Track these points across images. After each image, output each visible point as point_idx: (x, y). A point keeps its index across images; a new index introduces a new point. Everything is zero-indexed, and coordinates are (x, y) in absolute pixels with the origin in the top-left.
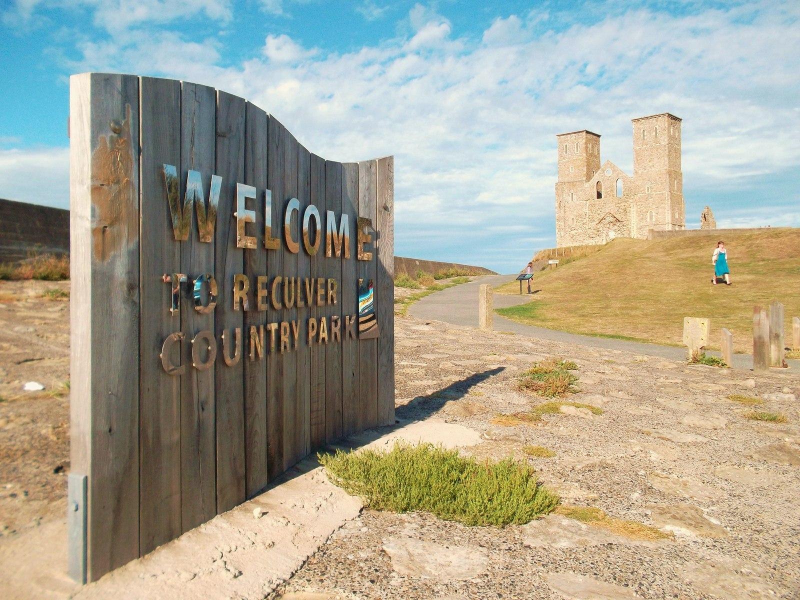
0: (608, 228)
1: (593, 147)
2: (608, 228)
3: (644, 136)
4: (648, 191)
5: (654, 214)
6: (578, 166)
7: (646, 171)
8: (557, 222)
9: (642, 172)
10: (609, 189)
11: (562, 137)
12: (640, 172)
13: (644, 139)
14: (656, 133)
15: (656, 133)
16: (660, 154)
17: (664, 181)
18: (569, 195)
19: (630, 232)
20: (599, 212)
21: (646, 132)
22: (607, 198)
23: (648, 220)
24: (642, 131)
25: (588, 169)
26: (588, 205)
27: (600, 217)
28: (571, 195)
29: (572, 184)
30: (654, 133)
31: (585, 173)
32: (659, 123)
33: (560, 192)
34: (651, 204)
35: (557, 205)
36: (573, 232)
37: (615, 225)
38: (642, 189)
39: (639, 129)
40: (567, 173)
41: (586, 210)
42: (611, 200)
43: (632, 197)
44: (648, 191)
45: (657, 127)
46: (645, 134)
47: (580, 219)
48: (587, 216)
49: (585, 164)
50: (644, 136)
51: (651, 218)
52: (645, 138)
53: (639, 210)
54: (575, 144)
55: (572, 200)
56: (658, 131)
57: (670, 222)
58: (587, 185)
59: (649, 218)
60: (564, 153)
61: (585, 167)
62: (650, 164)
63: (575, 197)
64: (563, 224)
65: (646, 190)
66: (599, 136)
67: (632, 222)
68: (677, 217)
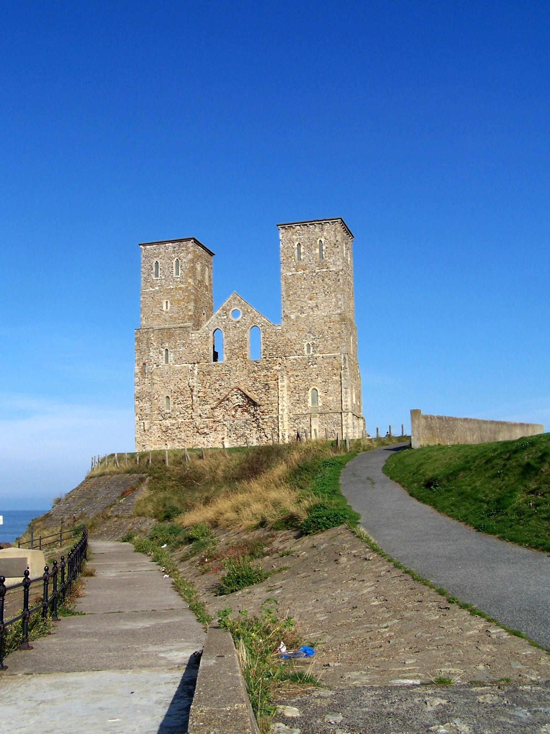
0: (233, 416)
1: (203, 270)
2: (233, 416)
3: (299, 253)
4: (309, 351)
5: (319, 394)
7: (303, 316)
8: (137, 403)
9: (297, 317)
10: (237, 345)
11: (148, 247)
12: (293, 317)
13: (299, 259)
14: (321, 250)
15: (321, 250)
16: (330, 286)
18: (160, 352)
23: (310, 404)
24: (296, 246)
25: (196, 308)
26: (196, 372)
27: (219, 396)
28: (164, 353)
29: (167, 334)
30: (318, 251)
33: (144, 346)
34: (314, 375)
35: (137, 369)
36: (168, 422)
38: (298, 347)
39: (291, 241)
40: (157, 311)
41: (194, 382)
42: (240, 364)
43: (280, 360)
45: (323, 240)
46: (302, 251)
47: (181, 398)
48: (195, 393)
50: (299, 253)
51: (315, 401)
52: (302, 257)
53: (291, 385)
54: (174, 262)
55: (167, 361)
56: (324, 248)
57: (350, 410)
58: (194, 336)
59: (310, 400)
60: (153, 276)
61: (192, 304)
62: (312, 303)
63: (171, 356)
64: (147, 405)
65: (305, 349)
67: (280, 407)
68: (354, 402)
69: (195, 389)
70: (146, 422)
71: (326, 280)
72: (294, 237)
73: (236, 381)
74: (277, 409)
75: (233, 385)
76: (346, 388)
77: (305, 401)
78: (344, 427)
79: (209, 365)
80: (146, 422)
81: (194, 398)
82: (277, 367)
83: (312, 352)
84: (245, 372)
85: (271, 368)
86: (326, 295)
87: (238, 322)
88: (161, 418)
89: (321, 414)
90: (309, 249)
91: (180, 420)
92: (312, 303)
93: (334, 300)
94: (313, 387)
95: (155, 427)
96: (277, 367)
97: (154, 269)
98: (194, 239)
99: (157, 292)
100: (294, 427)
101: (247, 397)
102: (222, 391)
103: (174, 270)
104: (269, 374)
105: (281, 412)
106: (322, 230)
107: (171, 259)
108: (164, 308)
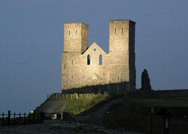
3: (116, 31)
6: (77, 44)
14: (122, 30)
15: (122, 30)
17: (126, 59)
20: (88, 73)
21: (117, 29)
22: (94, 65)
24: (115, 28)
30: (121, 30)
31: (81, 48)
32: (124, 25)
45: (123, 27)
46: (117, 30)
49: (81, 43)
50: (116, 31)
52: (116, 32)
55: (72, 64)
56: (123, 29)
58: (81, 56)
60: (68, 35)
63: (74, 62)
69: (81, 73)
71: (124, 40)
72: (114, 25)
75: (94, 73)
86: (123, 45)
92: (119, 48)
97: (69, 32)
103: (75, 33)
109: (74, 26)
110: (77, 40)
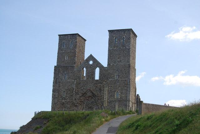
3: (115, 41)
4: (116, 78)
9: (113, 65)
14: (123, 40)
16: (126, 54)
19: (103, 104)
36: (63, 101)
37: (92, 98)
44: (116, 78)
45: (124, 37)
48: (74, 91)
50: (115, 41)
56: (125, 40)
63: (67, 77)
66: (85, 40)
67: (105, 98)
70: (56, 100)
73: (89, 87)
74: (103, 98)
75: (88, 88)
76: (129, 92)
77: (114, 96)
78: (127, 106)
79: (80, 81)
80: (56, 100)
81: (74, 92)
82: (104, 83)
83: (117, 78)
84: (93, 84)
85: (102, 83)
87: (92, 65)
88: (61, 99)
89: (119, 101)
90: (119, 40)
91: (68, 100)
93: (127, 59)
94: (117, 91)
95: (59, 102)
96: (104, 83)
98: (78, 34)
99: (63, 53)
100: (109, 105)
101: (93, 93)
102: (84, 90)
104: (101, 85)
105: (105, 100)
106: (125, 33)
107: (69, 41)
108: (66, 59)
109: (69, 38)
110: (72, 52)
